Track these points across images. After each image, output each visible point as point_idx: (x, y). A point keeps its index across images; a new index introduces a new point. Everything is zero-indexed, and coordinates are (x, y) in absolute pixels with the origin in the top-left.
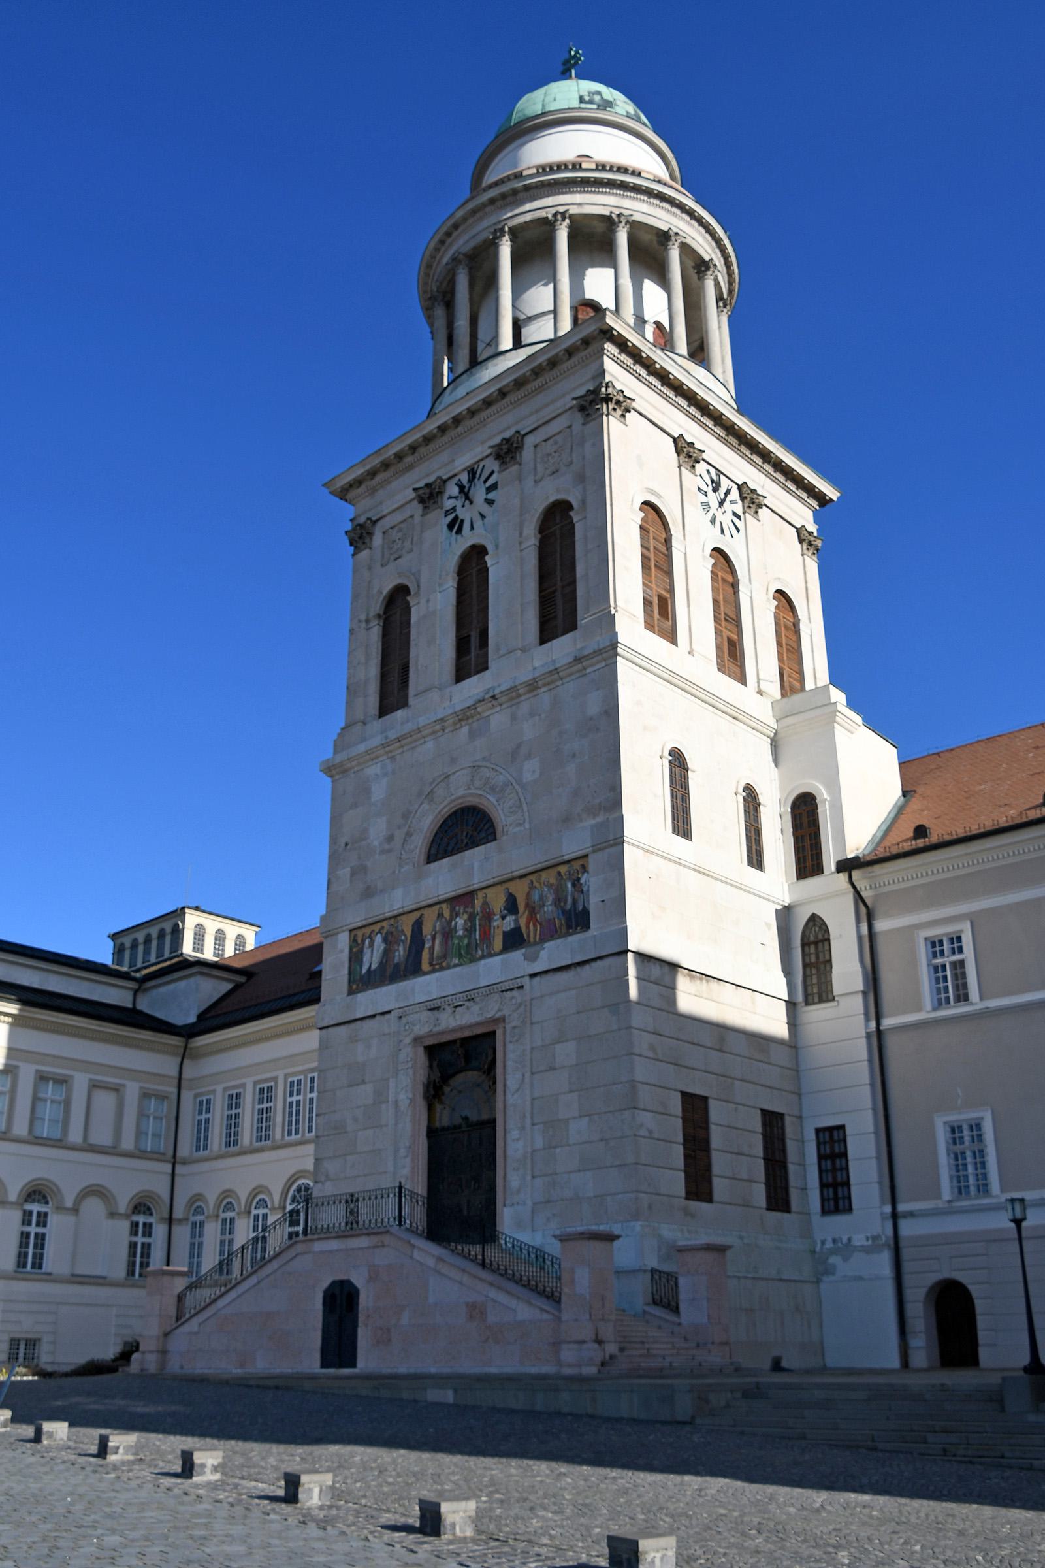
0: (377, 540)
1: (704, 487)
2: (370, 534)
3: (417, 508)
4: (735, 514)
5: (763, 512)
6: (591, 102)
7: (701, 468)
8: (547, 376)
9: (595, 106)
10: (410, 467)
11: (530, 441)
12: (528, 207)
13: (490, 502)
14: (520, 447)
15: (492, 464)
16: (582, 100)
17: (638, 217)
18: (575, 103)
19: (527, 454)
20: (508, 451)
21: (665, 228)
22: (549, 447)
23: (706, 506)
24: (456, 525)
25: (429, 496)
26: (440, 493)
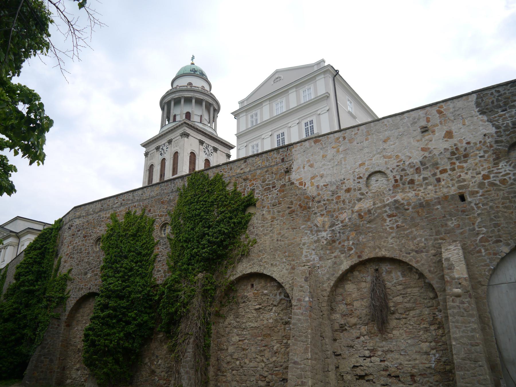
0: (149, 156)
1: (205, 148)
2: (148, 154)
3: (155, 150)
4: (211, 152)
5: (218, 152)
6: (192, 71)
7: (205, 144)
8: (177, 129)
9: (193, 72)
10: (155, 143)
11: (173, 140)
12: (177, 94)
13: (167, 151)
14: (172, 142)
15: (167, 144)
16: (191, 71)
17: (197, 97)
18: (189, 72)
19: (173, 143)
20: (170, 142)
21: (202, 98)
22: (176, 142)
23: (205, 152)
24: (161, 154)
25: (158, 148)
26: (159, 148)
